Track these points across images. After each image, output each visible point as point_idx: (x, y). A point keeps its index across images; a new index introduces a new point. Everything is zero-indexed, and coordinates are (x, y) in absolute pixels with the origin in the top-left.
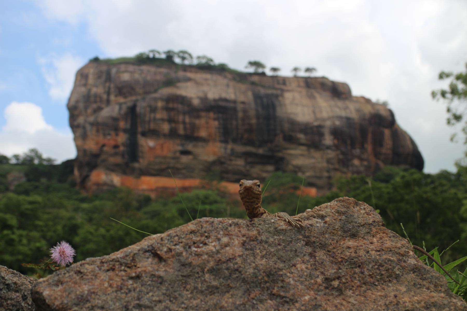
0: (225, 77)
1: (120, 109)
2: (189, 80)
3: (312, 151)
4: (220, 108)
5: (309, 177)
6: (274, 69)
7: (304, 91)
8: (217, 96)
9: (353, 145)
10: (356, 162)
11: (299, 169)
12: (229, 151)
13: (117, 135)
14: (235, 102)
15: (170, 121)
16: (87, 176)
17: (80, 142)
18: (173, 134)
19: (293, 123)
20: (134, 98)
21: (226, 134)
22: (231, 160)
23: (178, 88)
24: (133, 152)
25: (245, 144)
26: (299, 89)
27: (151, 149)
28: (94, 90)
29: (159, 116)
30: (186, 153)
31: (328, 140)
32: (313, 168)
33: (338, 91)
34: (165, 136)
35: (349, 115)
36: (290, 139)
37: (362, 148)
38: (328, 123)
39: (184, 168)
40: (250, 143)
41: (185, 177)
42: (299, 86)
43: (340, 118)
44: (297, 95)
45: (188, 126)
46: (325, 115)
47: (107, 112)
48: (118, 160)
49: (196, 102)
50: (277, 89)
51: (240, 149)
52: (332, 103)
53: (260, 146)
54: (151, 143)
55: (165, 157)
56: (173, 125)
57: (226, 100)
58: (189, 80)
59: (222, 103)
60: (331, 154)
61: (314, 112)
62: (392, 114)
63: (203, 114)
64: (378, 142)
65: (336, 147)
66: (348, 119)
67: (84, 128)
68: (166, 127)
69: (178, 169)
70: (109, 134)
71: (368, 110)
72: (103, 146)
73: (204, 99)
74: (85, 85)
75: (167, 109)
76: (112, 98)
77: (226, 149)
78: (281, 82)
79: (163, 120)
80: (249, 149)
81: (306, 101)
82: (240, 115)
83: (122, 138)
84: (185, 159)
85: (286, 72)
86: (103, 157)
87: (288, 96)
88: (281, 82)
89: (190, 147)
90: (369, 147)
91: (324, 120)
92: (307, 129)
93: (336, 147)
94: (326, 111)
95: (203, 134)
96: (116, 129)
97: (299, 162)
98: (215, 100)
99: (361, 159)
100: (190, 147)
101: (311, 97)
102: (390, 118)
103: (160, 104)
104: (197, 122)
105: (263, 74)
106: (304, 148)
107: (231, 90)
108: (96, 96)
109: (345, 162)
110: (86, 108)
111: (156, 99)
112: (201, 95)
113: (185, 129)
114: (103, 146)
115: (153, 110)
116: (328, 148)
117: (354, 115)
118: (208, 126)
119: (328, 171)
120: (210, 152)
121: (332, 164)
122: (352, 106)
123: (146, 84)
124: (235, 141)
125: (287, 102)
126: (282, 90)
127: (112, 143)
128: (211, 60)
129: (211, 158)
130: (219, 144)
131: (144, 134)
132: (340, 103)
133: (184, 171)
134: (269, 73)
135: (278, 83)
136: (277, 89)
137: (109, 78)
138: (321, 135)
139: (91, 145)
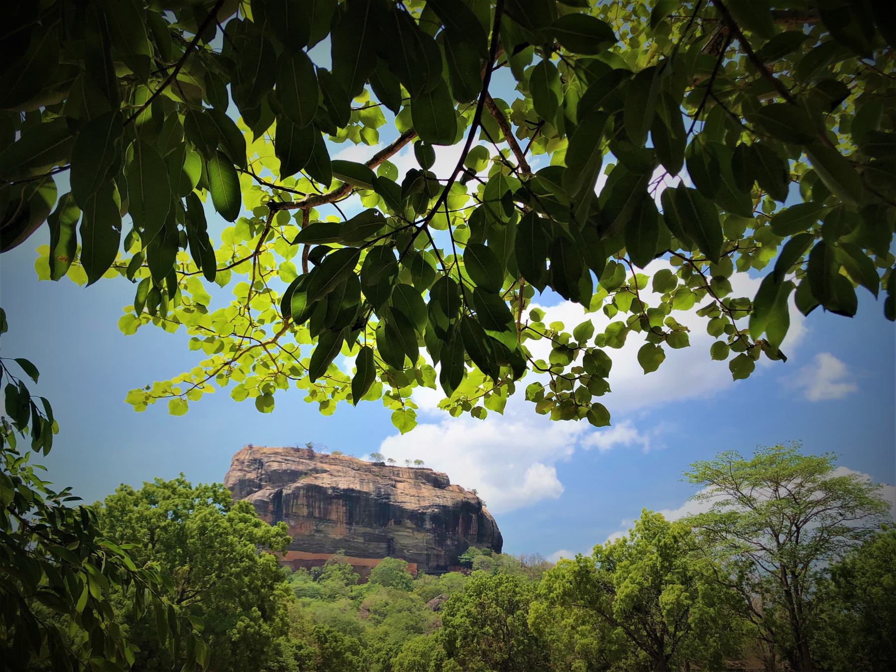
2: (326, 471)
3: (416, 533)
4: (349, 497)
5: (412, 554)
6: (391, 460)
7: (412, 481)
8: (346, 487)
11: (405, 547)
14: (359, 492)
19: (403, 511)
21: (351, 519)
22: (354, 538)
25: (365, 526)
30: (318, 531)
31: (428, 525)
32: (415, 546)
33: (439, 482)
36: (398, 523)
43: (438, 506)
46: (427, 503)
47: (258, 495)
49: (330, 492)
51: (361, 530)
57: (352, 490)
59: (348, 493)
60: (430, 536)
62: (479, 504)
63: (335, 501)
64: (467, 527)
66: (444, 507)
68: (305, 511)
71: (460, 498)
75: (307, 496)
77: (350, 529)
80: (368, 530)
81: (413, 491)
84: (318, 536)
85: (400, 463)
90: (460, 530)
93: (433, 531)
95: (334, 517)
97: (405, 542)
100: (322, 527)
103: (302, 492)
105: (382, 465)
107: (357, 481)
108: (250, 480)
109: (440, 541)
110: (241, 490)
111: (298, 488)
112: (334, 485)
113: (320, 512)
117: (449, 503)
118: (338, 511)
120: (337, 532)
124: (357, 523)
126: (396, 481)
130: (345, 526)
132: (439, 492)
134: (387, 464)
138: (423, 521)
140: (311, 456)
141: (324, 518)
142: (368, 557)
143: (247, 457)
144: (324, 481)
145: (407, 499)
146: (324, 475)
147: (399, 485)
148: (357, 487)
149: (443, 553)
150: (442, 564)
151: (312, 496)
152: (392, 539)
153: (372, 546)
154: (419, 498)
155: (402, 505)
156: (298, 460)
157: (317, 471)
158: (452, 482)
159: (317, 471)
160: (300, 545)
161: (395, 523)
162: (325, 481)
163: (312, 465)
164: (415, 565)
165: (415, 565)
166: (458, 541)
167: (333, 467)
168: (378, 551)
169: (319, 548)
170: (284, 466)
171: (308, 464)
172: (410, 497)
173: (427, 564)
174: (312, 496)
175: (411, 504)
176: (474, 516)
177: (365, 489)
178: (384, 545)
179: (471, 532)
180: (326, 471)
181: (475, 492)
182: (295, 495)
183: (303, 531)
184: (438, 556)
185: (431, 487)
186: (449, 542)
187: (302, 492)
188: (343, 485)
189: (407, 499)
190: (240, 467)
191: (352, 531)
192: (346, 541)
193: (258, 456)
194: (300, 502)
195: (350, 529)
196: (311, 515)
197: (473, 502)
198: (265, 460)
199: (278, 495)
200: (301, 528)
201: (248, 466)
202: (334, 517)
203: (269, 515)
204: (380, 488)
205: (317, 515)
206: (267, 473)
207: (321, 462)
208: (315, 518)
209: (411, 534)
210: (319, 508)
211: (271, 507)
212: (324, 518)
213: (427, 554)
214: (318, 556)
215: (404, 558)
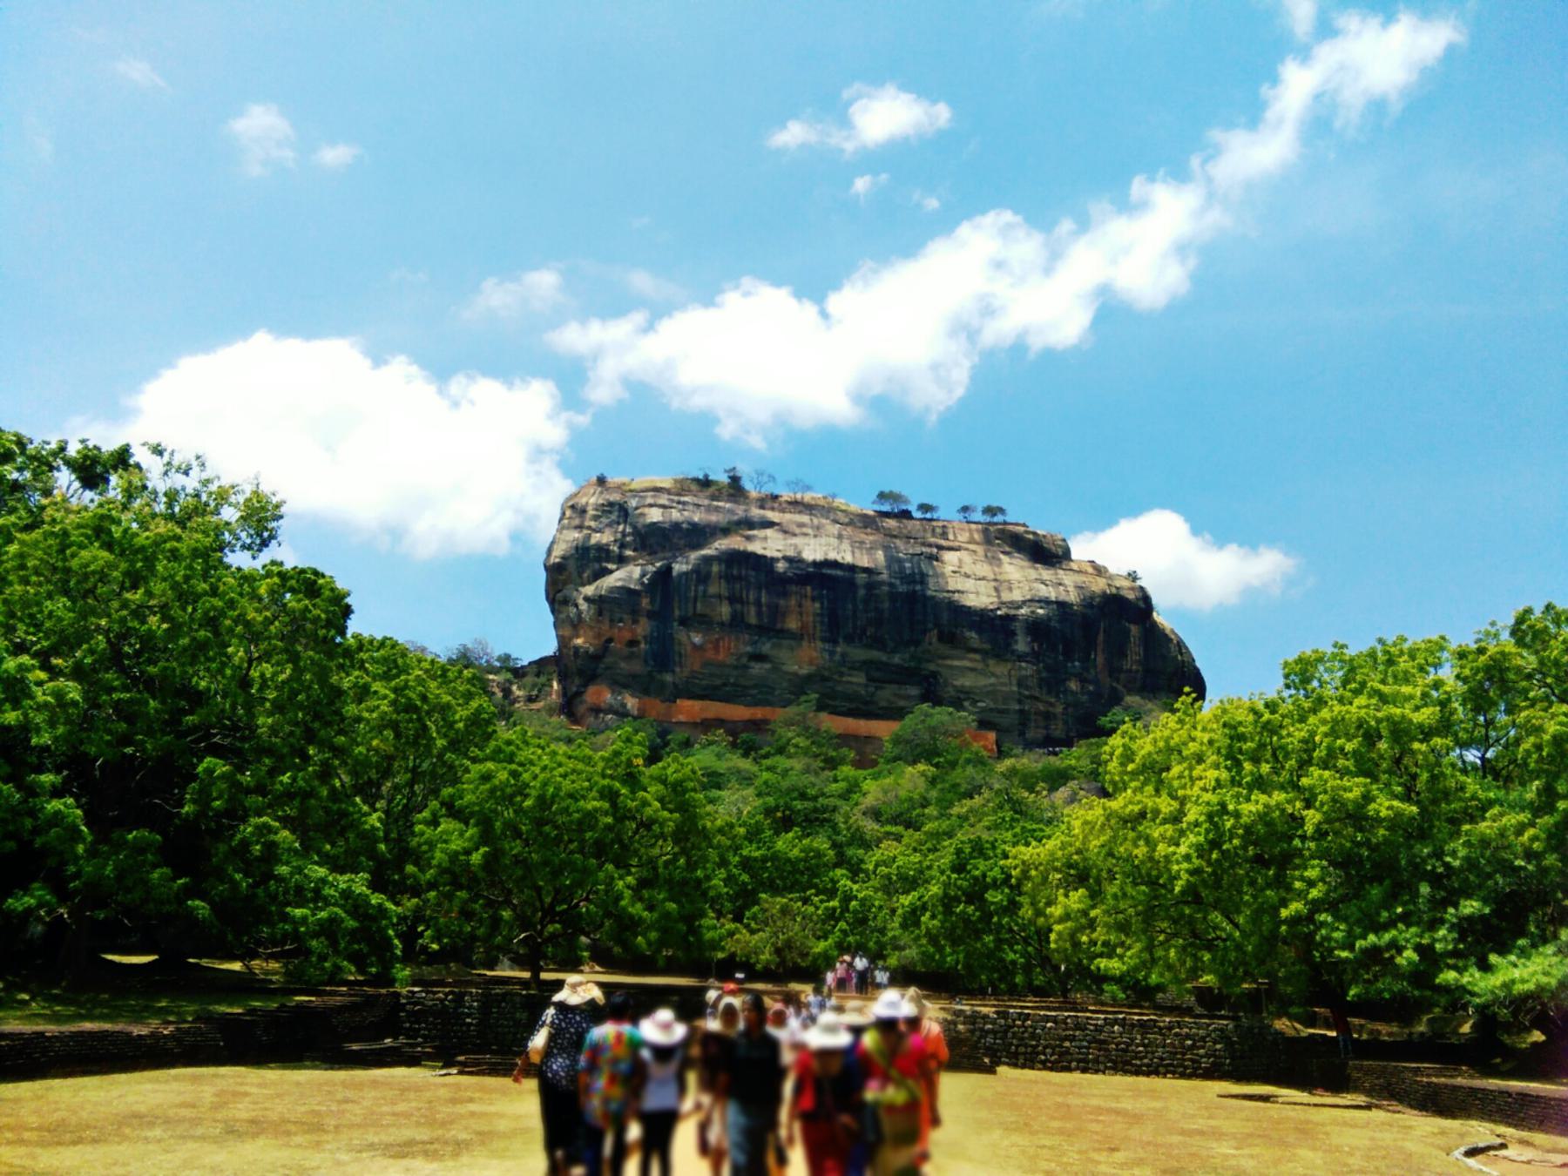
0: (836, 522)
1: (643, 575)
3: (991, 662)
4: (825, 579)
6: (925, 508)
7: (980, 549)
8: (819, 557)
9: (1068, 655)
10: (1073, 685)
12: (837, 657)
13: (635, 622)
14: (852, 568)
15: (732, 600)
16: (579, 694)
18: (737, 623)
21: (834, 628)
22: (842, 674)
23: (748, 538)
24: (663, 654)
25: (869, 647)
27: (694, 646)
28: (596, 538)
29: (713, 590)
30: (759, 658)
31: (1022, 645)
32: (991, 693)
34: (722, 624)
35: (1063, 597)
36: (951, 639)
37: (1086, 659)
39: (755, 686)
40: (877, 643)
41: (756, 704)
46: (1017, 596)
47: (619, 577)
48: (637, 667)
49: (781, 566)
50: (930, 545)
51: (859, 654)
52: (1033, 574)
53: (894, 651)
55: (721, 665)
56: (738, 607)
57: (835, 564)
60: (1027, 669)
61: (996, 589)
62: (1146, 598)
63: (794, 588)
64: (1118, 649)
65: (1034, 657)
66: (1062, 605)
68: (725, 611)
69: (745, 687)
70: (621, 620)
71: (1099, 585)
72: (610, 640)
74: (580, 527)
75: (728, 577)
77: (832, 653)
78: (938, 530)
79: (720, 597)
80: (875, 654)
81: (984, 569)
82: (862, 592)
83: (643, 628)
84: (757, 669)
86: (608, 660)
88: (938, 530)
89: (766, 648)
90: (1100, 660)
93: (1034, 657)
94: (1020, 584)
95: (793, 624)
96: (635, 613)
97: (966, 681)
98: (815, 564)
99: (1083, 681)
101: (993, 560)
102: (1142, 605)
103: (715, 568)
104: (782, 602)
105: (906, 515)
106: (978, 657)
107: (846, 545)
109: (1053, 682)
112: (791, 553)
113: (759, 614)
114: (610, 640)
116: (1021, 657)
117: (1073, 597)
118: (802, 612)
119: (1020, 702)
120: (802, 659)
121: (1027, 688)
122: (1069, 580)
124: (849, 639)
125: (948, 569)
126: (940, 548)
127: (627, 636)
129: (804, 671)
130: (819, 644)
131: (684, 622)
132: (1047, 574)
136: (930, 545)
140: (735, 488)
141: (771, 629)
143: (592, 500)
144: (769, 545)
145: (969, 585)
146: (769, 532)
147: (949, 556)
148: (848, 558)
149: (1059, 709)
150: (1058, 730)
151: (740, 578)
152: (934, 675)
153: (886, 695)
154: (999, 584)
156: (706, 502)
157: (749, 524)
159: (749, 524)
160: (716, 688)
161: (941, 638)
162: (770, 543)
163: (740, 511)
165: (992, 736)
166: (1096, 682)
167: (788, 516)
169: (762, 694)
170: (675, 515)
171: (730, 511)
173: (1022, 734)
174: (740, 578)
175: (978, 596)
176: (1134, 630)
179: (1127, 665)
180: (769, 524)
181: (1133, 576)
182: (700, 574)
183: (721, 657)
184: (1048, 716)
185: (1026, 564)
187: (715, 568)
188: (813, 551)
189: (969, 585)
190: (577, 522)
191: (837, 657)
192: (824, 679)
193: (615, 497)
194: (713, 590)
196: (737, 623)
197: (1131, 596)
198: (633, 503)
200: (716, 648)
201: (596, 518)
203: (644, 621)
204: (900, 561)
205: (753, 620)
206: (636, 532)
207: (762, 507)
208: (749, 626)
209: (980, 666)
210: (758, 603)
211: (645, 602)
212: (771, 629)
213: (1021, 712)
214: (758, 713)
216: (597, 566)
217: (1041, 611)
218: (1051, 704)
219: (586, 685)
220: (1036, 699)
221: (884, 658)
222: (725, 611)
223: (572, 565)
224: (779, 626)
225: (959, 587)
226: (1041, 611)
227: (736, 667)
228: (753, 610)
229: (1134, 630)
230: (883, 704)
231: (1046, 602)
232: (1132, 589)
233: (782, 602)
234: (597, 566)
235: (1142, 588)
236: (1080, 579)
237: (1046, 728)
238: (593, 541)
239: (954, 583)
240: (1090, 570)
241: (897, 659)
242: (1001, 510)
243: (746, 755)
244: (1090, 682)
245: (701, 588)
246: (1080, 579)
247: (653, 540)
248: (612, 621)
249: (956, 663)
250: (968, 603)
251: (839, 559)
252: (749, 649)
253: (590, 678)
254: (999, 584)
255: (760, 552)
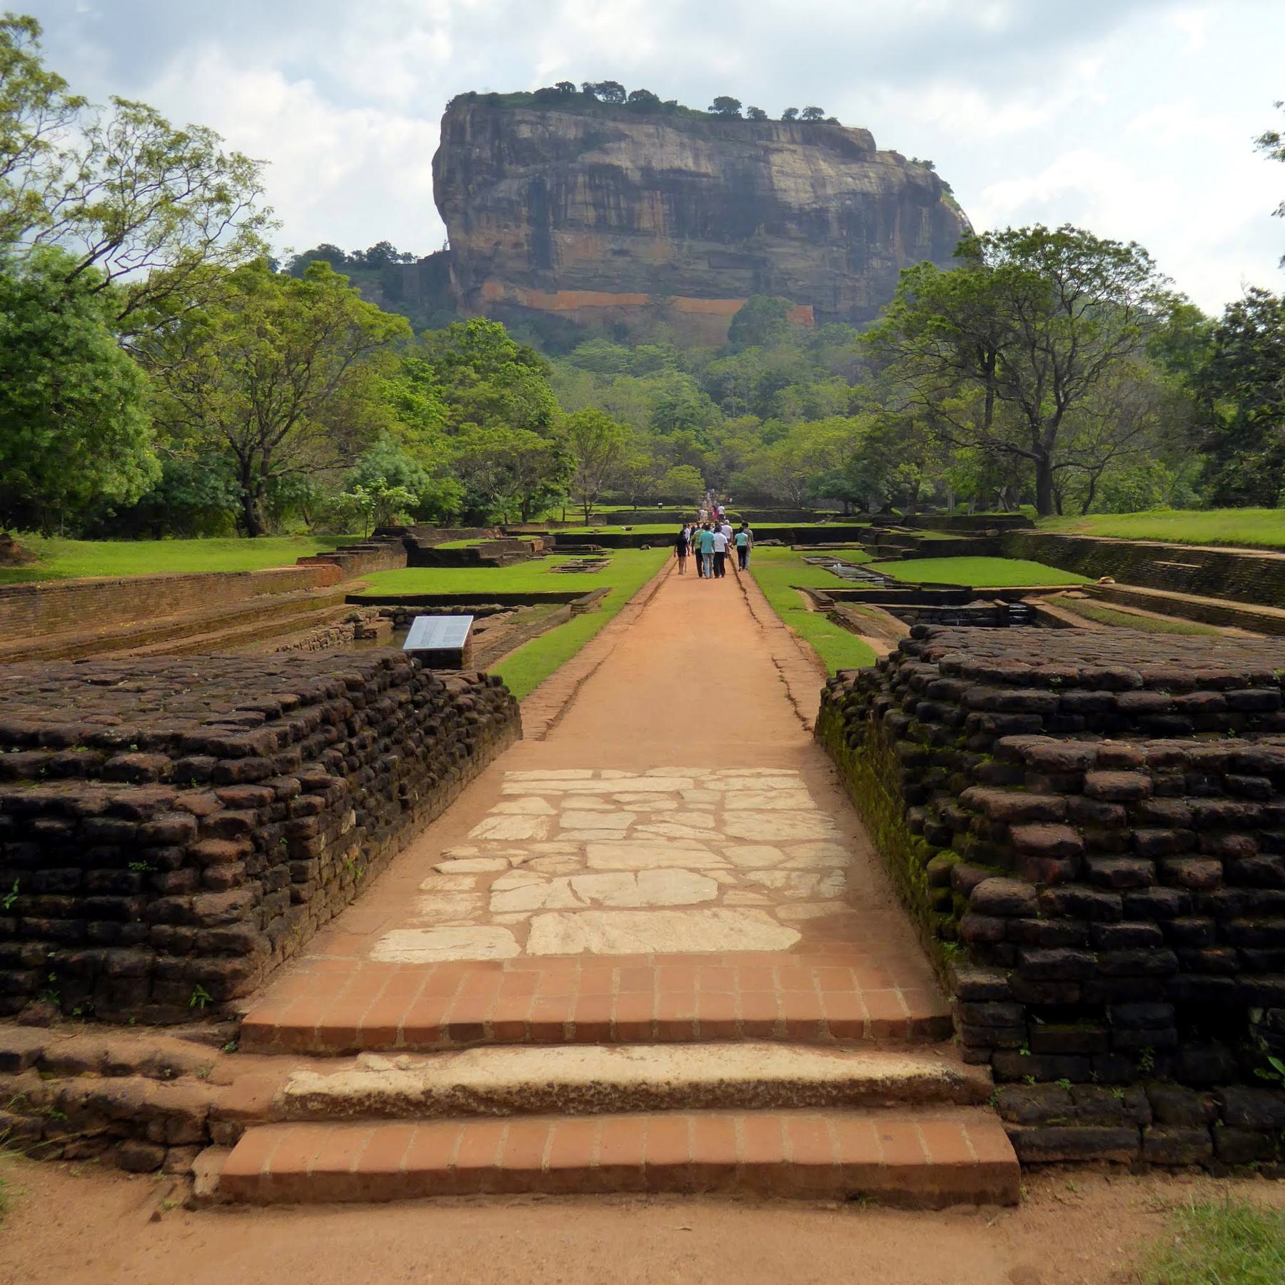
4: (672, 184)
7: (798, 148)
8: (666, 166)
10: (875, 263)
13: (518, 227)
14: (691, 174)
17: (461, 236)
18: (601, 225)
20: (539, 167)
21: (681, 225)
22: (688, 264)
23: (606, 152)
26: (791, 147)
27: (570, 247)
29: (579, 198)
30: (621, 253)
34: (588, 226)
36: (777, 231)
38: (833, 206)
42: (793, 141)
44: (787, 156)
45: (624, 213)
48: (520, 265)
49: (636, 176)
51: (702, 246)
54: (569, 239)
57: (679, 171)
58: (622, 137)
59: (671, 176)
63: (646, 193)
67: (466, 214)
68: (591, 214)
70: (506, 226)
71: (898, 176)
72: (498, 243)
73: (647, 171)
75: (594, 188)
76: (507, 166)
77: (680, 247)
83: (525, 230)
84: (620, 262)
85: (775, 114)
87: (776, 159)
90: (897, 238)
91: (827, 199)
92: (801, 216)
95: (646, 224)
100: (626, 243)
101: (808, 159)
103: (580, 179)
104: (637, 206)
106: (796, 244)
112: (642, 163)
113: (619, 217)
114: (498, 243)
115: (572, 189)
118: (652, 213)
120: (658, 251)
123: (558, 145)
128: (655, 99)
129: (659, 262)
130: (670, 239)
132: (855, 168)
133: (618, 281)
135: (760, 138)
137: (498, 133)
139: (480, 242)
141: (628, 226)
142: (717, 296)
146: (623, 145)
148: (689, 163)
150: (863, 303)
154: (818, 182)
155: (779, 195)
158: (882, 145)
164: (810, 308)
168: (738, 284)
172: (794, 176)
174: (598, 187)
176: (925, 211)
177: (706, 167)
178: (747, 274)
186: (875, 263)
187: (580, 179)
194: (579, 198)
195: (680, 247)
197: (920, 182)
199: (536, 188)
202: (646, 224)
203: (524, 225)
205: (614, 221)
207: (614, 120)
208: (610, 227)
211: (524, 210)
212: (628, 226)
215: (789, 295)
216: (480, 178)
217: (848, 202)
218: (857, 280)
219: (481, 282)
220: (844, 275)
221: (722, 248)
222: (591, 214)
223: (459, 177)
224: (636, 226)
225: (783, 185)
226: (848, 202)
227: (603, 262)
228: (613, 213)
229: (925, 211)
230: (723, 286)
231: (854, 193)
232: (926, 176)
233: (637, 206)
234: (480, 178)
235: (934, 176)
236: (882, 169)
237: (853, 299)
238: (474, 156)
239: (781, 183)
240: (891, 161)
241: (732, 249)
242: (821, 111)
243: (618, 340)
244: (888, 259)
245: (570, 197)
246: (882, 169)
247: (524, 152)
248: (498, 227)
249: (779, 250)
250: (790, 200)
251: (684, 168)
252: (612, 246)
253: (483, 274)
254: (818, 182)
255: (616, 163)
